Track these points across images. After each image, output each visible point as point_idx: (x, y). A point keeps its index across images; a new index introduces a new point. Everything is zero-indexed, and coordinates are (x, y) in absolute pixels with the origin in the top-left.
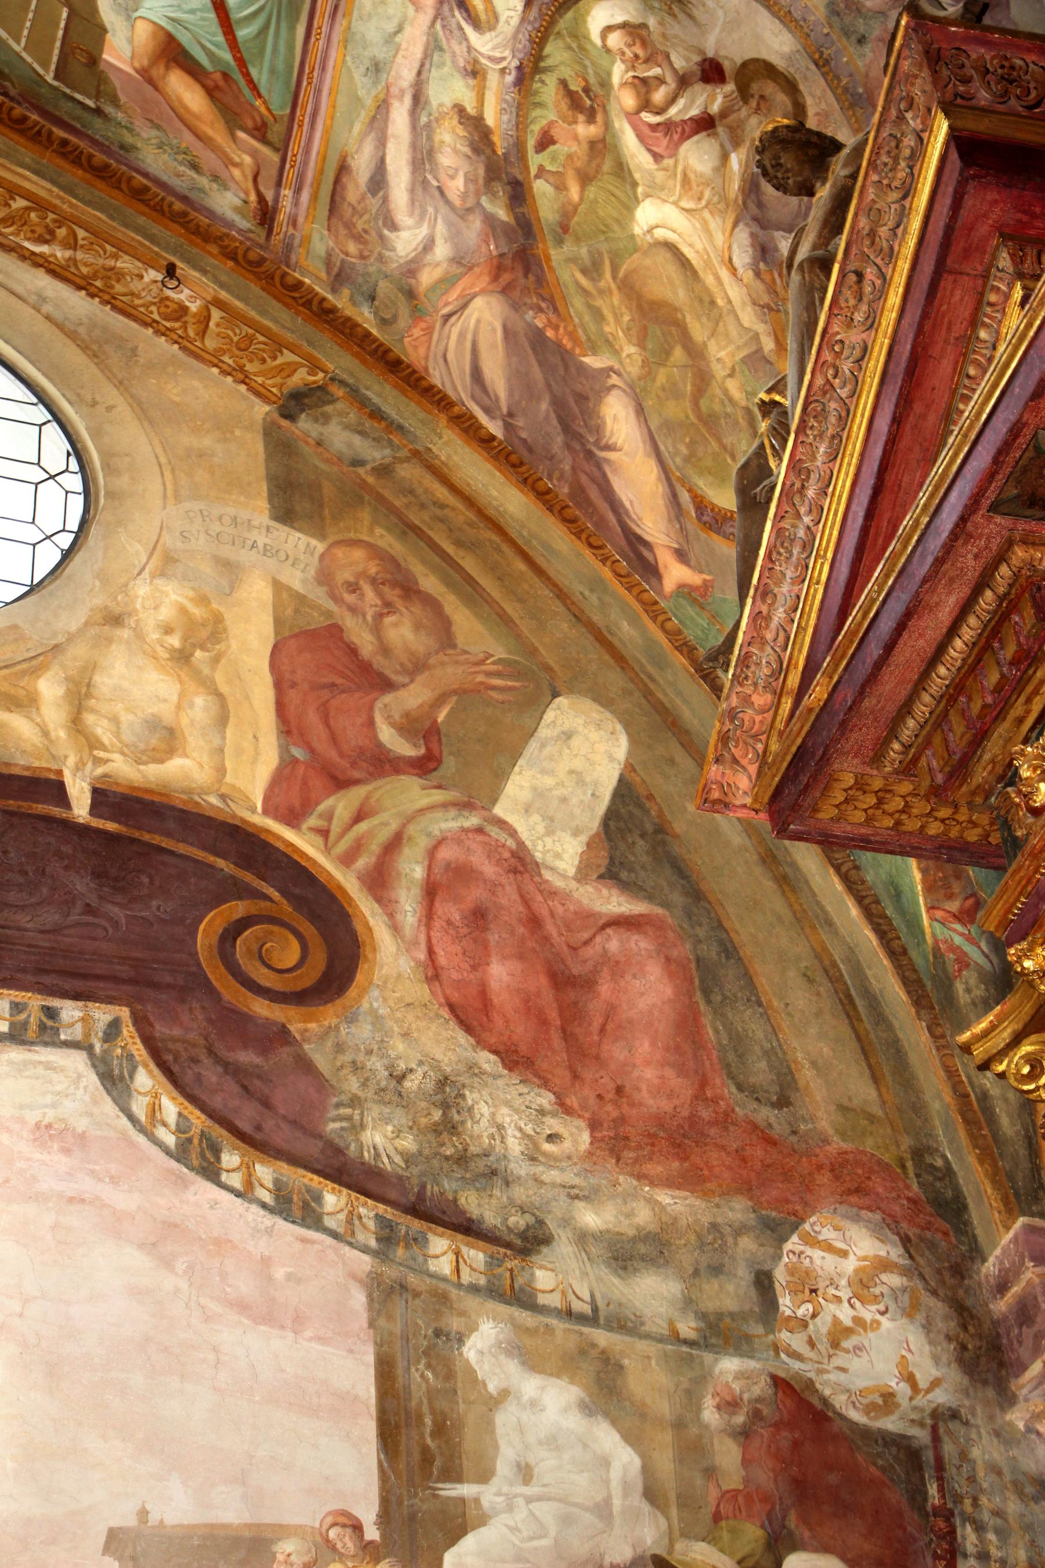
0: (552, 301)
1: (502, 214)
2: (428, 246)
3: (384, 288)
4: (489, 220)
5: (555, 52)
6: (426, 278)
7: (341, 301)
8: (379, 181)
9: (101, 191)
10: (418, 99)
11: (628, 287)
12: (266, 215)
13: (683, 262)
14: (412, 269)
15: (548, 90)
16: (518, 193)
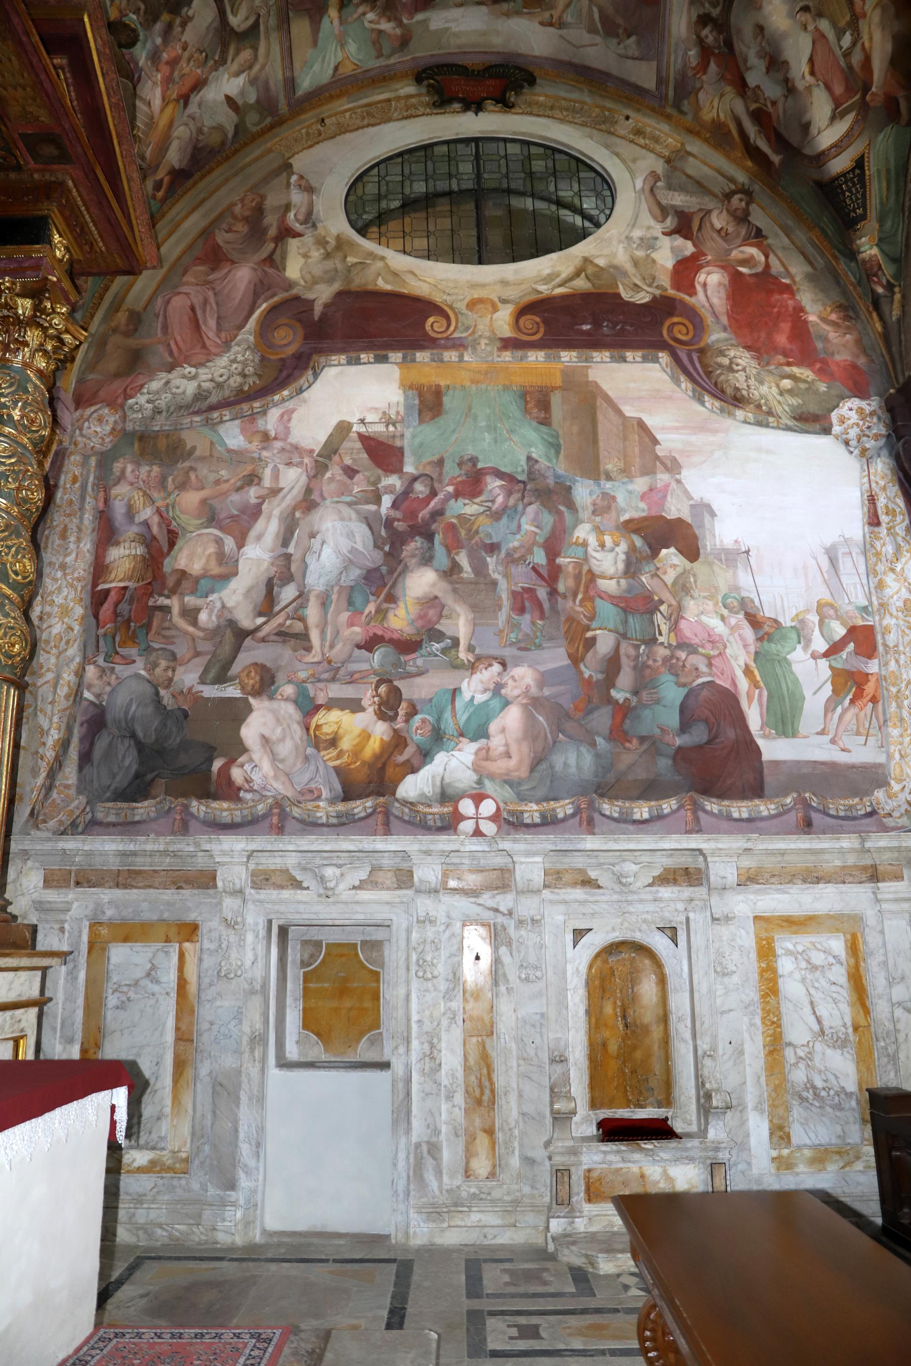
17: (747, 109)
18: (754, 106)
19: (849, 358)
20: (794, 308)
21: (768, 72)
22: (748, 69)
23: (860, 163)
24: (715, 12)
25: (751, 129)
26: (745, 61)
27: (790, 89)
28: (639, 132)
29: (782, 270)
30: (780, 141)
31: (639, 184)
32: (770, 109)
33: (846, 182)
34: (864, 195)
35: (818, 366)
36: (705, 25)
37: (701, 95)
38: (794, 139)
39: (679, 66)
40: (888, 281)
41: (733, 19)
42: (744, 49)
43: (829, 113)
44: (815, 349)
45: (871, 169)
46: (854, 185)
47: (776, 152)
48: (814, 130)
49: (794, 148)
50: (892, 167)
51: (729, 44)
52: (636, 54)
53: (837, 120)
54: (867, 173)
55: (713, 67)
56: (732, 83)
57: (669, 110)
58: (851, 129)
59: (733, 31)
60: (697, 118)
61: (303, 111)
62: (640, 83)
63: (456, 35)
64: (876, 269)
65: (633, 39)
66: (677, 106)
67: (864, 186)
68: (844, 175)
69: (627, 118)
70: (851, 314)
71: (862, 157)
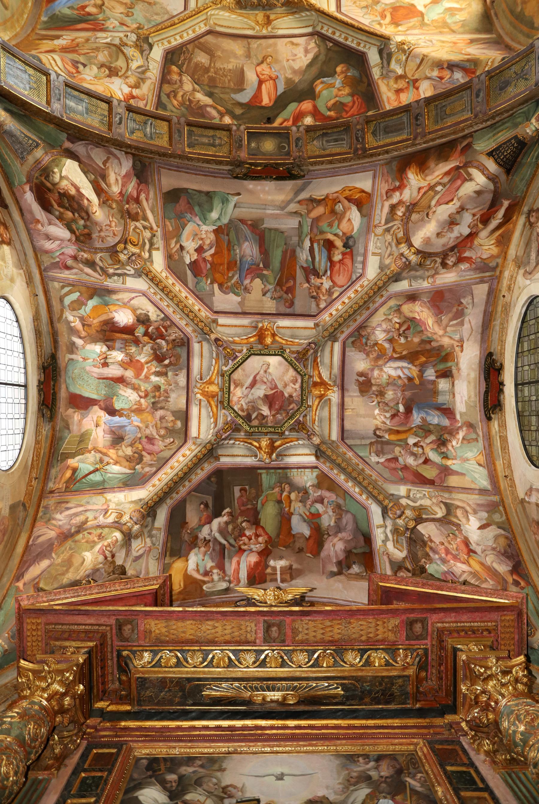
0: (61, 544)
1: (73, 531)
2: (60, 520)
3: (48, 515)
4: (70, 529)
5: (106, 530)
6: (54, 522)
7: (41, 509)
8: (68, 509)
9: (45, 464)
10: (86, 511)
11: (71, 556)
12: (52, 492)
13: (83, 563)
14: (54, 519)
15: (99, 531)
16: (78, 532)
17: (483, 229)
18: (480, 226)
21: (457, 224)
22: (461, 235)
23: (490, 154)
24: (439, 260)
25: (494, 223)
26: (457, 238)
27: (462, 209)
28: (509, 288)
30: (494, 204)
31: (528, 282)
32: (478, 216)
33: (499, 157)
36: (447, 264)
37: (484, 257)
38: (489, 197)
39: (472, 273)
41: (439, 250)
42: (452, 240)
47: (502, 205)
48: (478, 188)
49: (494, 196)
51: (452, 249)
52: (470, 297)
55: (467, 254)
56: (472, 242)
57: (498, 273)
59: (445, 248)
60: (498, 256)
61: (499, 488)
62: (486, 293)
63: (469, 397)
65: (462, 301)
66: (494, 269)
67: (500, 146)
69: (504, 296)
71: (488, 154)
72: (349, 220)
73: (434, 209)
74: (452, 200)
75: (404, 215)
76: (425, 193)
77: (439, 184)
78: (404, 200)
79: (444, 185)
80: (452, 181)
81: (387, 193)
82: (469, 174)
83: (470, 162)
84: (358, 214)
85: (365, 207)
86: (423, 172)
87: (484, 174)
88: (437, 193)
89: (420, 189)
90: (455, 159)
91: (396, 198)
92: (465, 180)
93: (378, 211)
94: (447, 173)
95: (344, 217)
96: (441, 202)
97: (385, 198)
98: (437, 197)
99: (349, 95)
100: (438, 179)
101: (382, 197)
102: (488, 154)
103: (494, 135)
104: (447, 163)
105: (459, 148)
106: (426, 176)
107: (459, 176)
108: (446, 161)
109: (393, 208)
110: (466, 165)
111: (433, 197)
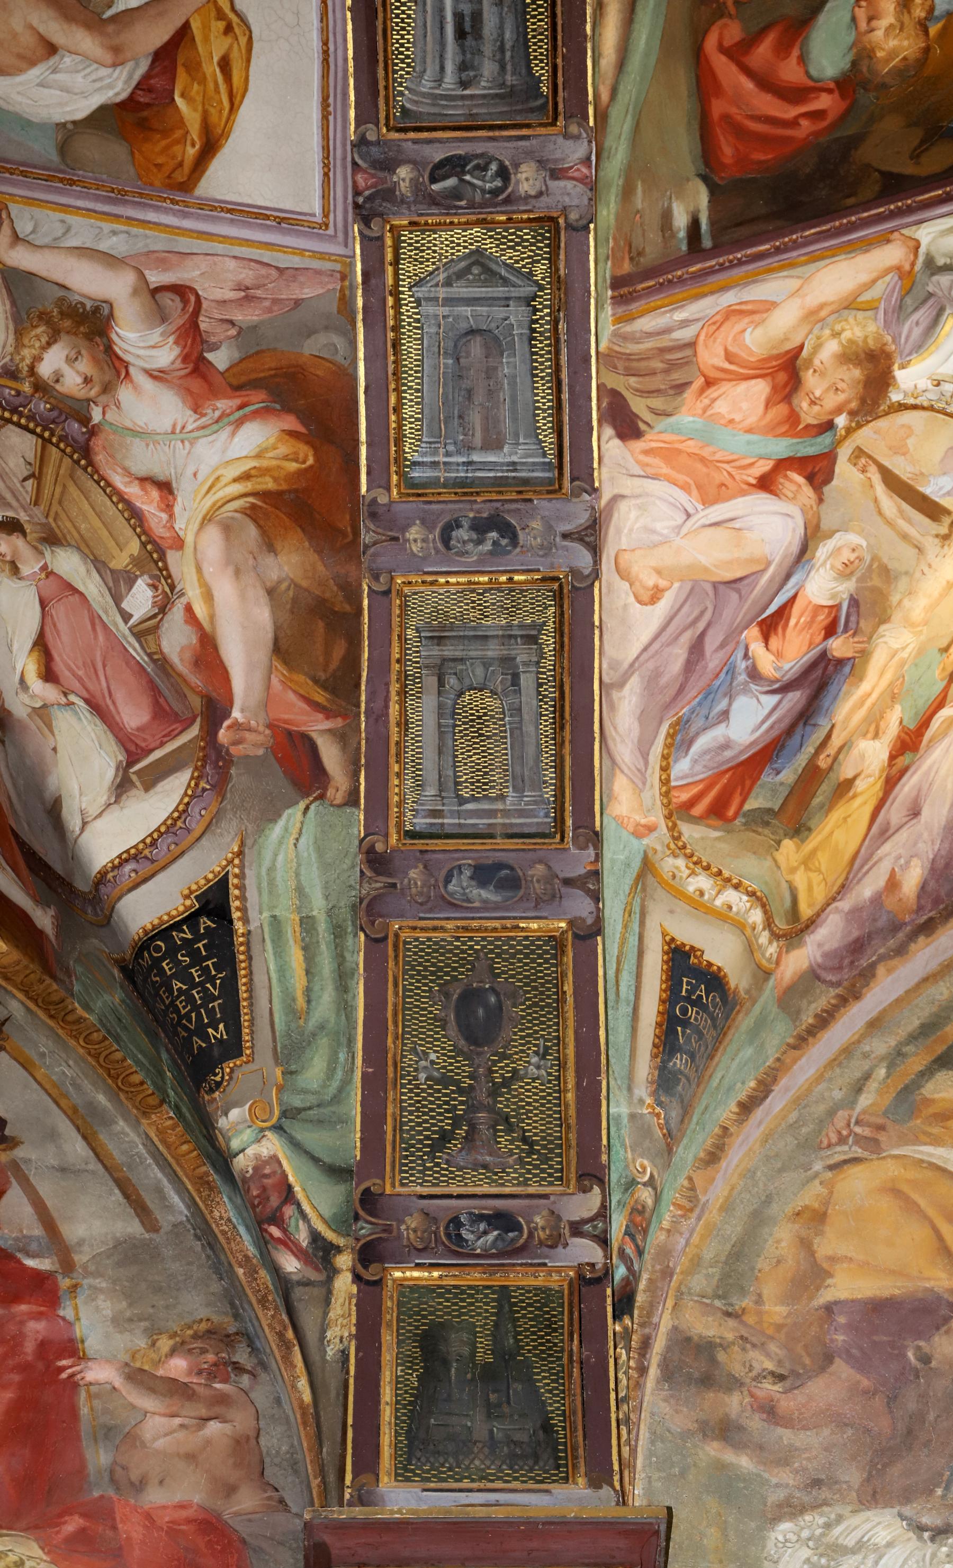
19: (197, 1499)
20: (43, 1346)
23: (215, 904)
29: (38, 1231)
34: (230, 989)
35: (72, 1525)
40: (315, 1237)
43: (110, 773)
44: (81, 1470)
45: (254, 913)
46: (197, 959)
47: (39, 901)
50: (318, 906)
53: (137, 792)
54: (239, 926)
58: (182, 812)
64: (274, 1201)
67: (228, 962)
68: (164, 932)
70: (242, 1356)
71: (222, 884)
72: (51, 49)
73: (30, 567)
74: (49, 675)
75: (41, 387)
76: (135, 515)
77: (163, 607)
78: (124, 393)
79: (146, 631)
80: (158, 679)
81: (180, 291)
82: (152, 778)
83: (221, 785)
84: (82, 108)
85: (118, 150)
86: (252, 513)
87: (131, 856)
88: (119, 584)
89: (165, 487)
90: (268, 700)
91: (144, 343)
92: (133, 750)
93: (84, 231)
94: (207, 651)
95: (68, 16)
96: (59, 612)
97: (155, 278)
98: (92, 587)
99: (862, 55)
100: (193, 594)
101: (162, 260)
102: (222, 884)
103: (307, 923)
104: (263, 653)
105: (319, 728)
106: (227, 529)
107: (166, 716)
108: (278, 649)
109: (91, 324)
110: (214, 763)
111: (99, 564)
